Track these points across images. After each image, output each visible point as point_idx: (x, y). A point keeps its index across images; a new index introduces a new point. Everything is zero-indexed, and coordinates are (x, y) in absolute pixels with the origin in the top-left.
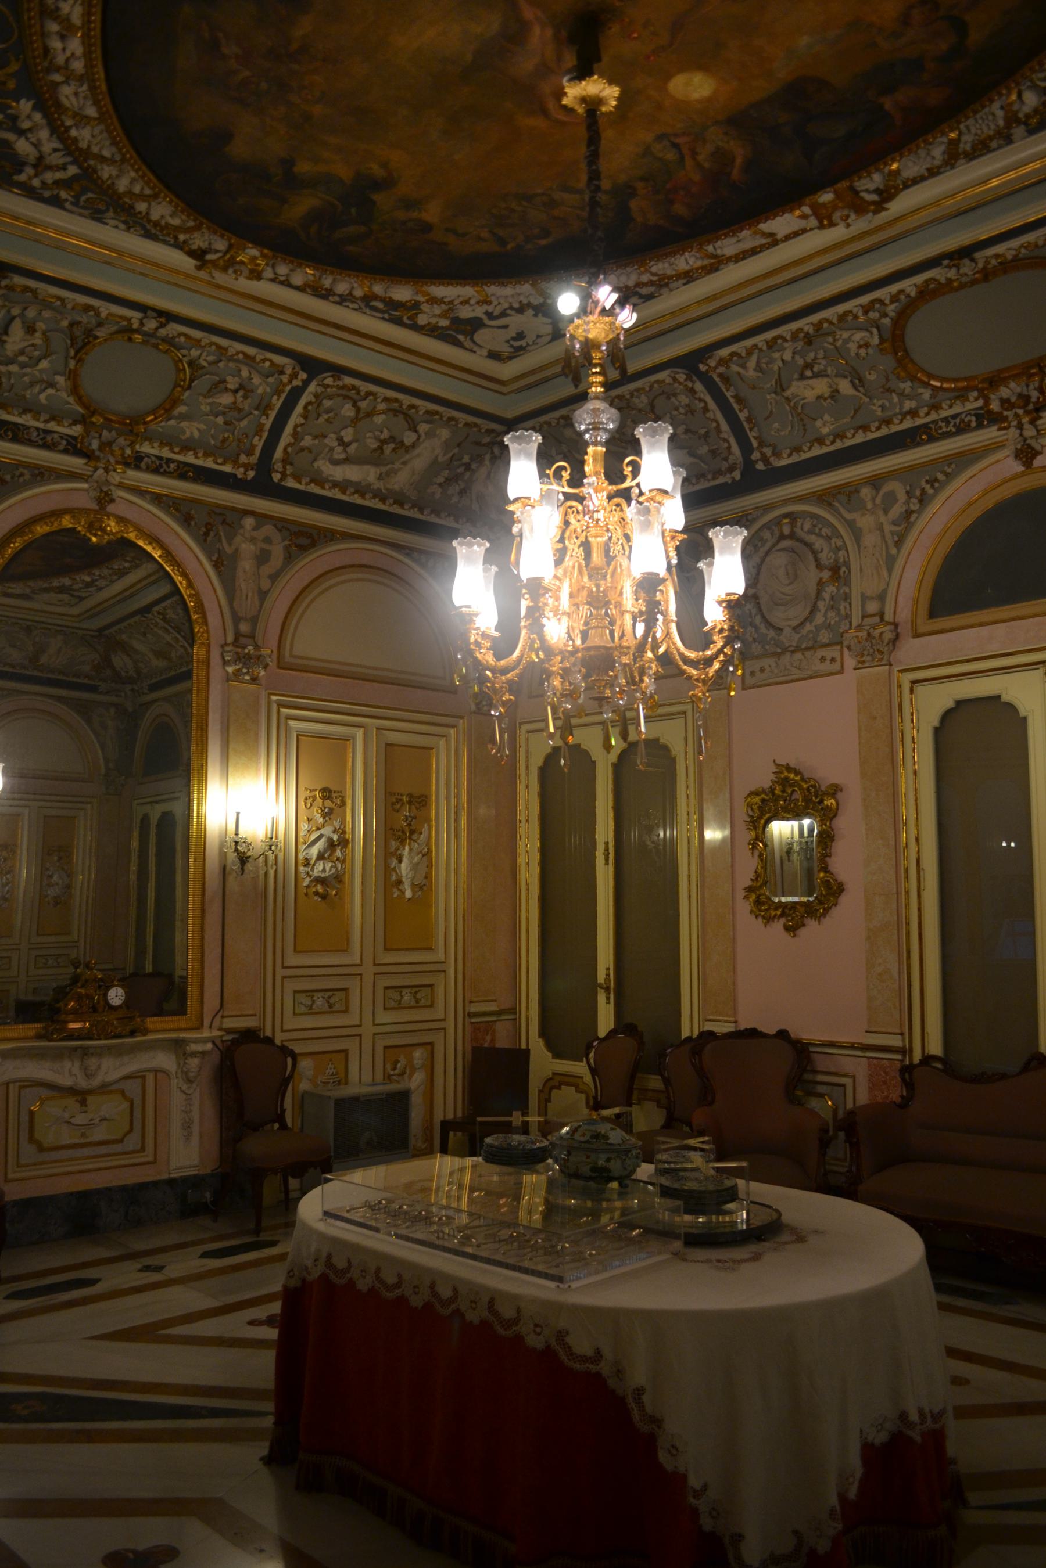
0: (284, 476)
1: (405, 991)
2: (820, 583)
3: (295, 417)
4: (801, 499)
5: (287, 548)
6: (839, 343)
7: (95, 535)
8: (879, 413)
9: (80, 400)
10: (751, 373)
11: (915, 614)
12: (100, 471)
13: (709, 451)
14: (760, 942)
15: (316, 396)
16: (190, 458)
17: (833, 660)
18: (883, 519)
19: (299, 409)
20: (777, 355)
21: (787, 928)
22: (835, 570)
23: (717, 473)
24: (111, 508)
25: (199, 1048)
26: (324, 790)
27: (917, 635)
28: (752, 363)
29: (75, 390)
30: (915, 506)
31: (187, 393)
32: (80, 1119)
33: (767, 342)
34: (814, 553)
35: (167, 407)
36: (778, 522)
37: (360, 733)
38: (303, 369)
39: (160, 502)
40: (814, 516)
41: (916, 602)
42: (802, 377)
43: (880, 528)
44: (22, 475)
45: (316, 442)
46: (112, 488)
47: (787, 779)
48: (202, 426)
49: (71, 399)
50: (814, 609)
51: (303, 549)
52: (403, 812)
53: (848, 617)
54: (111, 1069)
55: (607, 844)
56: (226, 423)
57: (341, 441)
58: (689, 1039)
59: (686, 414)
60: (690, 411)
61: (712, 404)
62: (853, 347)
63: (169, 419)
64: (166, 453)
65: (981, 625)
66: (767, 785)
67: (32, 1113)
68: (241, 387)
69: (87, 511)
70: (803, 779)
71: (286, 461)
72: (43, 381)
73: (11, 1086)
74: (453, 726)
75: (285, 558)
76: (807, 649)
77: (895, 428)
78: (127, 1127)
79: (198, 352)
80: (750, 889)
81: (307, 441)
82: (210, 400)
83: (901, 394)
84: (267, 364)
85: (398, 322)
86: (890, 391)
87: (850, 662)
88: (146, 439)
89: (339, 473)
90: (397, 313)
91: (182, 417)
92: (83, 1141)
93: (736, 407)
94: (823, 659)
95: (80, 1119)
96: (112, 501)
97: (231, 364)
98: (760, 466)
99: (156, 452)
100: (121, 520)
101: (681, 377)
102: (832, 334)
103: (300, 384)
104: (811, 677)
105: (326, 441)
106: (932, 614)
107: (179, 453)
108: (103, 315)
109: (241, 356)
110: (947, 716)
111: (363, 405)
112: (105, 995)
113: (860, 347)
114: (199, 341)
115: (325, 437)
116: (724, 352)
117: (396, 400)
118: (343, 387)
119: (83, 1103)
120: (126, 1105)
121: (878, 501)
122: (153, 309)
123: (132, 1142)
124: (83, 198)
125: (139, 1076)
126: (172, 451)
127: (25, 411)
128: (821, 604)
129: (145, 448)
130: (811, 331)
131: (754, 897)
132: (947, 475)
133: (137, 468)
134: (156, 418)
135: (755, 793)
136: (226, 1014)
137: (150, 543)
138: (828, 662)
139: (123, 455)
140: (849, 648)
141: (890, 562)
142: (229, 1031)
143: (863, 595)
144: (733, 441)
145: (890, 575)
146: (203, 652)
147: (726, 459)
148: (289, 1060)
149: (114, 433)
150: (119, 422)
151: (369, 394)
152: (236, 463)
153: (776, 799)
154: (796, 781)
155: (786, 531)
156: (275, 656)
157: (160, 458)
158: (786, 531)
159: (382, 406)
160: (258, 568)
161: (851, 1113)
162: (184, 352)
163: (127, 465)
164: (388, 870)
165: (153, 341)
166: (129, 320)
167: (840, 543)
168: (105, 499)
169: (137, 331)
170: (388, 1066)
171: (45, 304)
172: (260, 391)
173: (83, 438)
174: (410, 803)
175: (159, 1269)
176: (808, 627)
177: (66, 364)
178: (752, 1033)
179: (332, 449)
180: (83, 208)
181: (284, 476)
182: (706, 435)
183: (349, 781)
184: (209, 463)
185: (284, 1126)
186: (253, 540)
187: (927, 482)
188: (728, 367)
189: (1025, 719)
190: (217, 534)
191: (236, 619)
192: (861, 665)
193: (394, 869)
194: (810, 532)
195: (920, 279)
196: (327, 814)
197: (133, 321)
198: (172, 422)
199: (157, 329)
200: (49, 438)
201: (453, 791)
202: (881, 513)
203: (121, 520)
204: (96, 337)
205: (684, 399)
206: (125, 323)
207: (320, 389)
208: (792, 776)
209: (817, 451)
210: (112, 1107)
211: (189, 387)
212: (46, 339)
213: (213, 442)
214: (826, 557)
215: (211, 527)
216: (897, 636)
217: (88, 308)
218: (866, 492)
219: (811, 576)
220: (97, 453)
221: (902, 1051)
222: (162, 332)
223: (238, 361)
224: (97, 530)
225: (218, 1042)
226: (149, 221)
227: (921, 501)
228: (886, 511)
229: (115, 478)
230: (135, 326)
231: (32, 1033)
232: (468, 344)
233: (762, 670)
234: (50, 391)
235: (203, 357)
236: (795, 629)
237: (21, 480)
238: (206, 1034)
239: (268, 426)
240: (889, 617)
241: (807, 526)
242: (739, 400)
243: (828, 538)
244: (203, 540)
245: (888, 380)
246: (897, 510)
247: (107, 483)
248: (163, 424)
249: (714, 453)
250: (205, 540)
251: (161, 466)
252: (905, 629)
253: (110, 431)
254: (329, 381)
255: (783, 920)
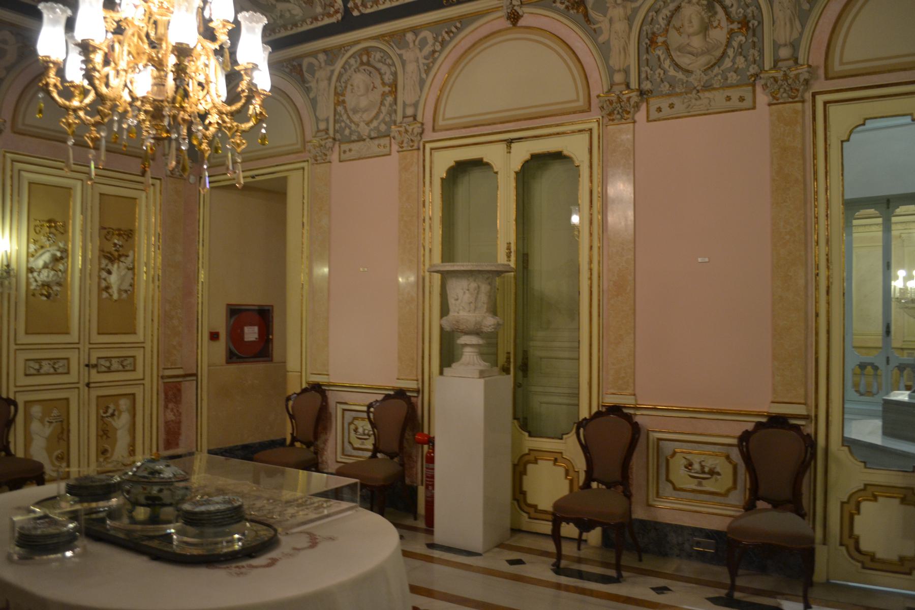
1: (114, 361)
34: (380, 74)
94: (379, 145)
121: (417, 43)
128: (383, 108)
145: (421, 91)
148: (12, 408)
155: (365, 58)
170: (101, 411)
193: (105, 279)
194: (380, 61)
218: (410, 36)
240: (419, 118)
243: (389, 65)
246: (427, 50)
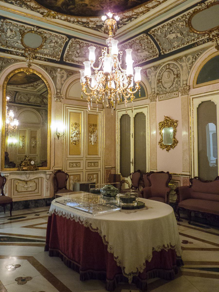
0: (66, 60)
2: (174, 78)
3: (67, 48)
4: (171, 60)
5: (67, 75)
6: (177, 25)
7: (27, 73)
8: (186, 40)
9: (23, 45)
10: (159, 33)
11: (193, 83)
12: (28, 60)
13: (152, 51)
14: (161, 153)
15: (71, 43)
16: (46, 57)
17: (177, 94)
18: (187, 64)
19: (68, 46)
20: (164, 29)
21: (167, 150)
22: (177, 75)
23: (154, 56)
24: (31, 67)
25: (49, 173)
26: (75, 123)
27: (194, 88)
28: (159, 31)
29: (22, 43)
30: (194, 60)
31: (45, 43)
32: (26, 186)
33: (162, 26)
34: (173, 72)
35: (41, 47)
36: (166, 66)
37: (83, 112)
38: (68, 38)
39: (41, 66)
40: (174, 64)
41: (194, 81)
42: (170, 34)
43: (187, 66)
44: (12, 61)
45: (72, 53)
46: (31, 63)
47: (167, 119)
48: (49, 50)
49: (21, 45)
50: (173, 84)
51: (70, 75)
52: (92, 127)
53: (180, 85)
54: (32, 177)
55: (132, 134)
56: (53, 50)
57: (77, 52)
58: (148, 173)
59: (147, 44)
60: (148, 43)
61: (152, 41)
62: (180, 26)
63: (41, 49)
64: (41, 56)
65: (207, 85)
66: (163, 121)
67: (16, 185)
68: (56, 42)
69: (26, 68)
70: (170, 119)
71: (66, 57)
72: (15, 42)
73: (12, 180)
74: (102, 110)
75: (67, 77)
76: (171, 92)
77: (190, 44)
78: (35, 188)
79: (46, 35)
80: (159, 142)
81: (70, 53)
82: (49, 45)
83: (191, 36)
84: (60, 37)
85: (85, 26)
86: (188, 35)
87: (180, 94)
88: (37, 53)
89: (77, 59)
90: (85, 24)
91: (44, 49)
92: (26, 191)
93: (157, 41)
94: (175, 94)
95: (26, 186)
96: (31, 66)
97: (53, 37)
98: (162, 54)
99: (39, 56)
100: (33, 70)
101: (145, 35)
102: (176, 23)
103: (67, 41)
104: (172, 98)
105: (74, 53)
106: (197, 83)
107: (44, 56)
108: (26, 27)
109: (55, 35)
110: (200, 105)
111: (81, 45)
112: (30, 162)
113: (182, 26)
114: (46, 32)
115: (74, 52)
116: (153, 29)
117: (88, 44)
118: (76, 41)
119: (26, 183)
120: (35, 184)
121: (186, 60)
122: (36, 26)
123: (36, 191)
124: (17, 2)
125: (38, 178)
126: (43, 55)
127: (12, 48)
128: (174, 82)
129: (37, 55)
130: (171, 23)
131: (160, 144)
132: (201, 53)
133: (36, 59)
134: (39, 49)
135: (161, 123)
136: (55, 167)
137: (39, 74)
138: (176, 95)
139: (32, 56)
140: (180, 91)
141: (189, 73)
142: (55, 170)
143: (183, 80)
144: (157, 49)
146: (50, 96)
147: (155, 53)
148: (67, 176)
149: (31, 52)
150: (31, 50)
151: (82, 42)
152: (56, 57)
153: (165, 123)
154: (169, 120)
155: (168, 67)
156: (65, 96)
157: (40, 57)
158: (168, 67)
159: (85, 45)
160: (61, 79)
161: (178, 188)
162: (43, 35)
163: (34, 58)
164: (88, 139)
165: (36, 33)
166: (31, 28)
167: (178, 69)
168: (30, 65)
169: (33, 31)
171: (14, 25)
172: (60, 42)
173: (24, 53)
174: (93, 126)
175: (38, 215)
176: (172, 87)
177: (20, 38)
178: (162, 172)
179: (76, 54)
180: (18, 4)
181: (66, 60)
182: (151, 48)
183: (80, 121)
184: (50, 58)
185: (66, 189)
186: (60, 73)
187: (197, 55)
188: (154, 33)
189: (216, 105)
190: (53, 72)
191: (57, 89)
192: (182, 95)
194: (173, 67)
195: (193, 9)
196: (76, 128)
197: (32, 28)
198: (42, 50)
199: (37, 30)
200: (18, 53)
201: (102, 123)
202: (187, 62)
203: (33, 70)
204: (25, 32)
205: (146, 40)
206: (30, 29)
207: (72, 42)
208: (168, 119)
209: (174, 50)
210: (32, 184)
211: (45, 42)
212: (15, 33)
213: (51, 53)
214: (176, 72)
215: (51, 71)
216: (190, 89)
217: (23, 26)
218: (184, 58)
219: (172, 76)
220: (27, 56)
221: (190, 176)
222: (38, 31)
223: (54, 36)
224: (28, 72)
225: (54, 172)
226: (31, 7)
227: (195, 59)
228: (188, 62)
229: (31, 61)
230: (32, 30)
231: (16, 170)
232: (100, 31)
233: (162, 97)
234: (17, 44)
235: (47, 36)
236: (169, 88)
237: (12, 62)
238: (51, 170)
239: (62, 50)
241: (172, 66)
242: (157, 40)
244: (50, 74)
245: (188, 33)
246: (190, 62)
247: (30, 62)
248: (40, 50)
249: (153, 52)
250: (50, 73)
251: (41, 59)
252: (191, 87)
253: (30, 52)
254: (73, 40)
255: (166, 149)
